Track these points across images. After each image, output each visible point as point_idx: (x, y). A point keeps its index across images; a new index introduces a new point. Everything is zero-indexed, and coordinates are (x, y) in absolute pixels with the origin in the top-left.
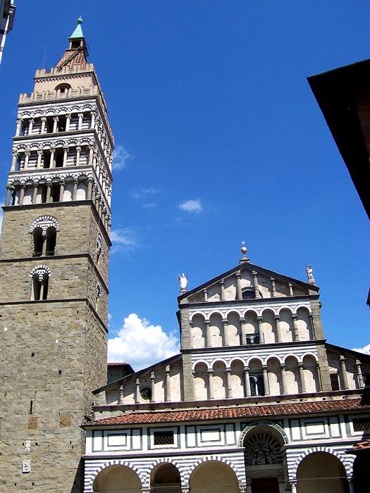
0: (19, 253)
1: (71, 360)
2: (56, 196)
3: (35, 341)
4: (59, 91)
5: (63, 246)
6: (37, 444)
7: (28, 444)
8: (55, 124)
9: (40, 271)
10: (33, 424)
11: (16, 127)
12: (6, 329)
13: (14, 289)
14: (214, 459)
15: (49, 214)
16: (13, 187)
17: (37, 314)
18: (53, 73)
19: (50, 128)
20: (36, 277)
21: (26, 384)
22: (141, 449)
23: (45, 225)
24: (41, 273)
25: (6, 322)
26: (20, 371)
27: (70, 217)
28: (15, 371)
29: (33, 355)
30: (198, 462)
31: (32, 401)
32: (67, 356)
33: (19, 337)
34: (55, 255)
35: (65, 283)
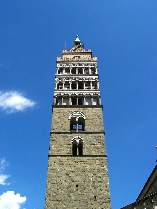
0: (63, 129)
2: (81, 102)
3: (77, 178)
5: (89, 127)
9: (78, 139)
12: (59, 170)
13: (62, 148)
15: (79, 111)
16: (57, 97)
17: (77, 163)
18: (71, 51)
21: (73, 204)
23: (78, 116)
24: (78, 141)
25: (58, 166)
26: (69, 196)
27: (91, 113)
28: (66, 196)
29: (77, 186)
33: (68, 175)
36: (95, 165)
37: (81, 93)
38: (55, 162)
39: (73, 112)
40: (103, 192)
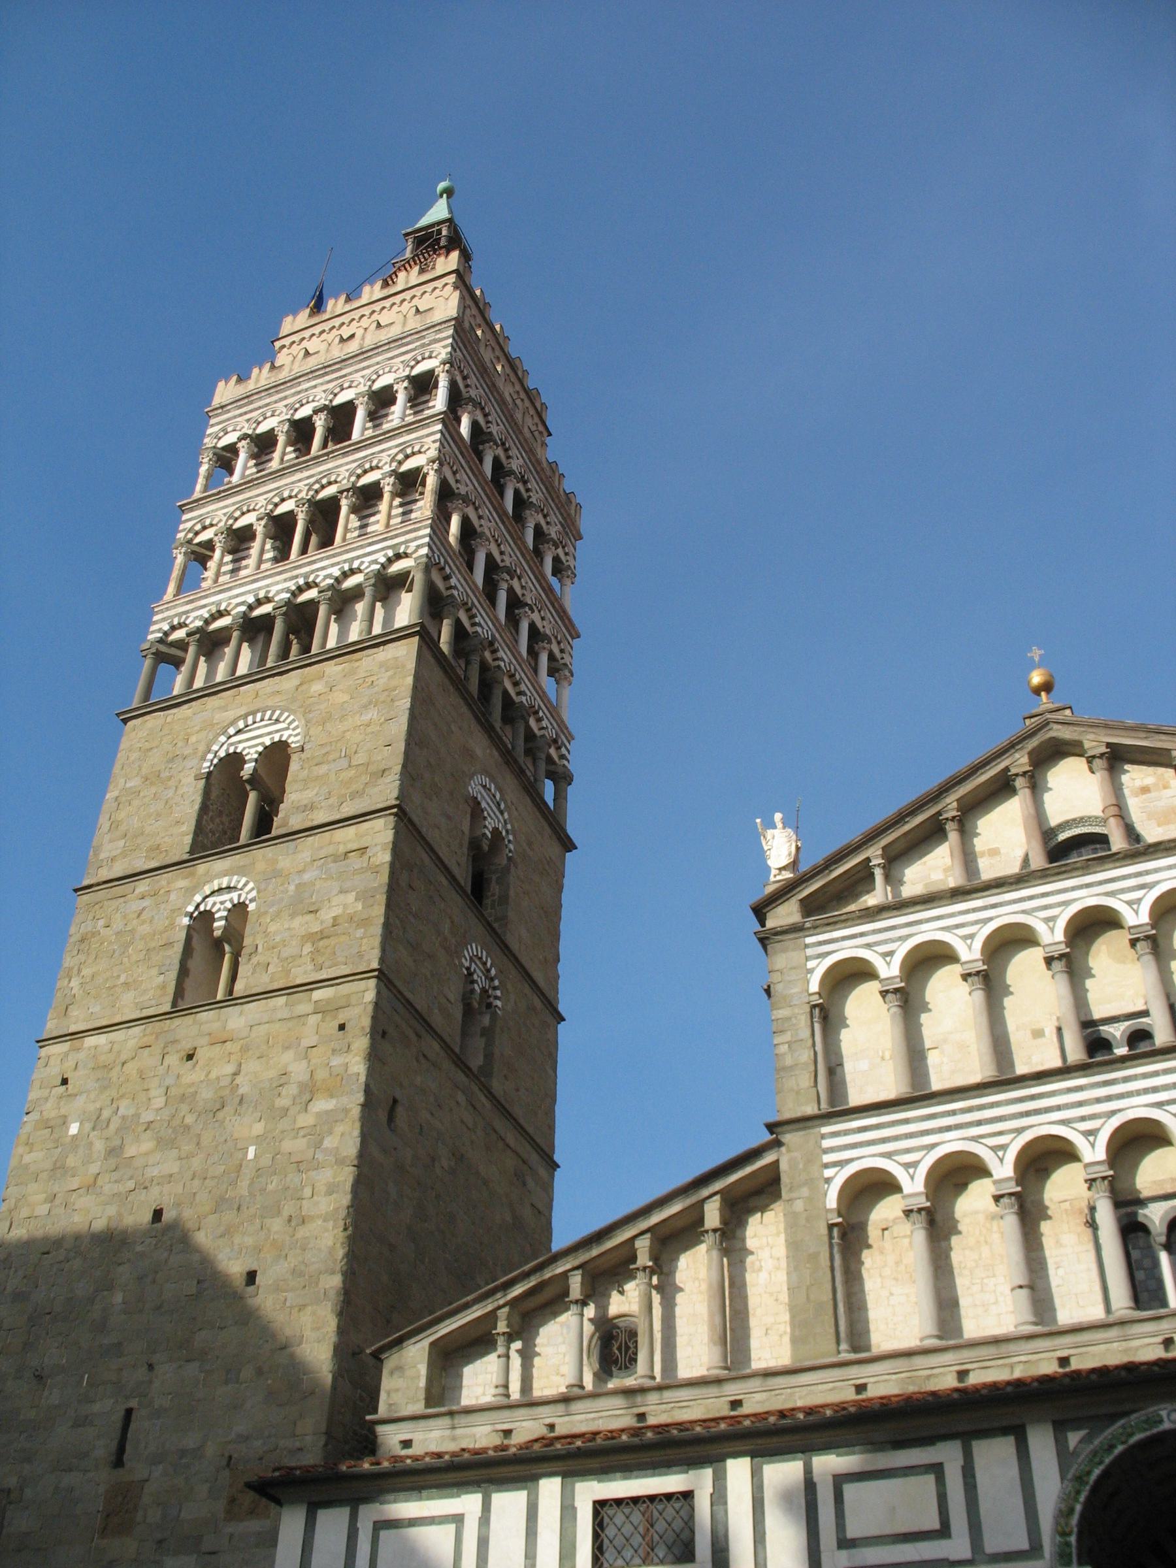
11: (198, 474)
12: (74, 1129)
17: (190, 1057)
24: (220, 906)
31: (129, 1412)
35: (301, 924)
36: (289, 1056)
37: (306, 576)
39: (233, 723)
40: (302, 1232)
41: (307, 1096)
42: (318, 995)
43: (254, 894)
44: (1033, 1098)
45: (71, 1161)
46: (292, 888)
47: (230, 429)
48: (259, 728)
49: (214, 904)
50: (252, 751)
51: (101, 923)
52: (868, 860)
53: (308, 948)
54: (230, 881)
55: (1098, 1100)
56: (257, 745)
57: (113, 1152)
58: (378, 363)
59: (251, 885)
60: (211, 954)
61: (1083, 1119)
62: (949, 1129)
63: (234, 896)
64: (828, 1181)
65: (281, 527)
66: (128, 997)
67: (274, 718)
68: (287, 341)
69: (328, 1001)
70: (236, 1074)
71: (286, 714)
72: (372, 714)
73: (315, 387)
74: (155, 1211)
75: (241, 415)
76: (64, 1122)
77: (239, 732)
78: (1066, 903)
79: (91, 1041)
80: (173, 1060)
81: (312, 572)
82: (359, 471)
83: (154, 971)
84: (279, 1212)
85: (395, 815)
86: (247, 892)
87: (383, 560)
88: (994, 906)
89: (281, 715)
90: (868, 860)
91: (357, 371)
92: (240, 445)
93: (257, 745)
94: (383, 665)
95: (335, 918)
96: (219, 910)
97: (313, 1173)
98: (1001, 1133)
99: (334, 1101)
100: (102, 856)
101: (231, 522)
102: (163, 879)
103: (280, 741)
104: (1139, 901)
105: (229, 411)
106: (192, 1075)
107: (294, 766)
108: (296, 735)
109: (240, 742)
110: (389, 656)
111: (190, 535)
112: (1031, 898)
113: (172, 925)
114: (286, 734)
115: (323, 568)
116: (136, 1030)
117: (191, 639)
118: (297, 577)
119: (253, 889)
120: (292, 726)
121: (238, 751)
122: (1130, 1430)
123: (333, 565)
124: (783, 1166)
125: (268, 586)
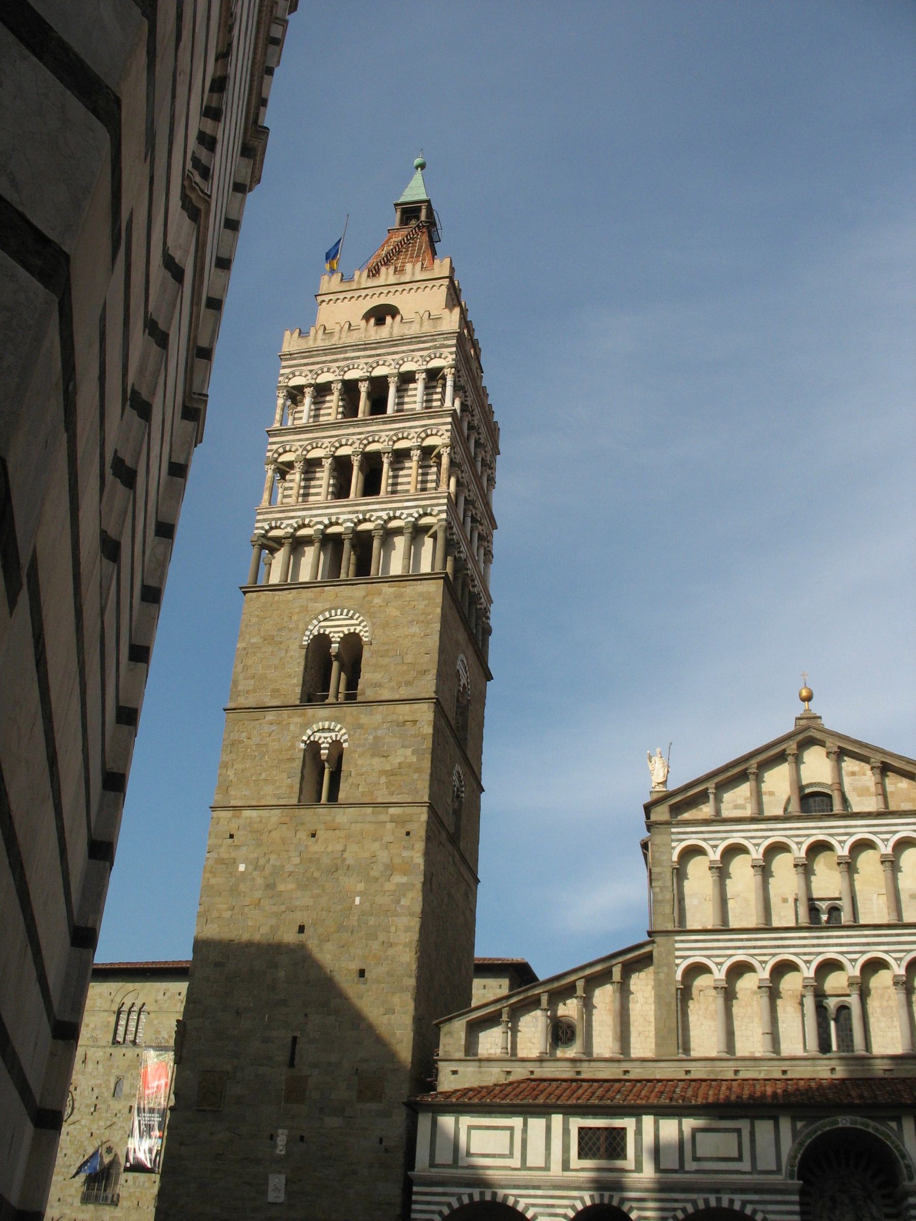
0: (275, 692)
1: (391, 945)
4: (372, 321)
6: (302, 1138)
7: (281, 1140)
8: (363, 396)
10: (296, 1091)
12: (242, 867)
13: (263, 776)
14: (725, 1204)
17: (313, 835)
18: (359, 283)
19: (350, 409)
20: (313, 747)
22: (547, 1168)
24: (326, 740)
30: (684, 1210)
31: (295, 1039)
32: (382, 937)
33: (270, 886)
34: (359, 699)
36: (376, 846)
37: (364, 513)
38: (232, 836)
39: (322, 613)
40: (391, 952)
41: (389, 872)
42: (392, 811)
43: (346, 737)
44: (782, 939)
45: (242, 887)
46: (371, 737)
47: (297, 373)
48: (339, 620)
49: (320, 738)
50: (336, 635)
51: (244, 735)
52: (707, 789)
53: (383, 780)
54: (330, 725)
55: (813, 946)
56: (339, 632)
57: (270, 886)
58: (403, 352)
59: (344, 731)
60: (323, 774)
61: (805, 954)
62: (739, 948)
63: (333, 734)
64: (677, 965)
65: (342, 466)
66: (268, 789)
67: (350, 615)
68: (326, 298)
69: (399, 816)
70: (344, 851)
71: (357, 615)
72: (415, 629)
73: (358, 358)
74: (300, 926)
75: (305, 365)
76: (234, 862)
77: (326, 620)
78: (808, 836)
79: (247, 813)
80: (303, 835)
81: (369, 511)
82: (395, 438)
83: (285, 775)
84: (376, 939)
85: (435, 703)
86: (342, 734)
87: (416, 515)
88: (771, 830)
89: (354, 614)
90: (707, 789)
91: (389, 354)
92: (307, 390)
93: (339, 632)
94: (421, 595)
95: (400, 763)
96: (323, 742)
97: (396, 919)
98: (765, 955)
99: (406, 878)
100: (240, 688)
101: (305, 453)
102: (285, 713)
103: (354, 632)
104: (844, 842)
105: (295, 359)
106: (316, 847)
107: (366, 654)
108: (366, 632)
109: (327, 627)
110: (425, 590)
111: (276, 455)
112: (791, 829)
113: (293, 747)
114: (358, 629)
115: (375, 510)
116: (277, 812)
117: (287, 541)
118: (357, 512)
119: (345, 734)
120: (363, 624)
121: (327, 633)
122: (824, 1126)
123: (382, 510)
124: (655, 954)
125: (338, 514)
